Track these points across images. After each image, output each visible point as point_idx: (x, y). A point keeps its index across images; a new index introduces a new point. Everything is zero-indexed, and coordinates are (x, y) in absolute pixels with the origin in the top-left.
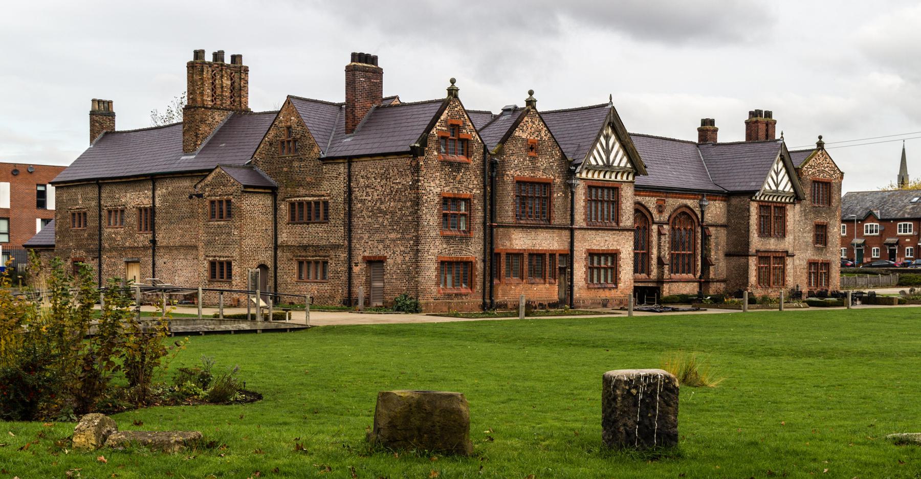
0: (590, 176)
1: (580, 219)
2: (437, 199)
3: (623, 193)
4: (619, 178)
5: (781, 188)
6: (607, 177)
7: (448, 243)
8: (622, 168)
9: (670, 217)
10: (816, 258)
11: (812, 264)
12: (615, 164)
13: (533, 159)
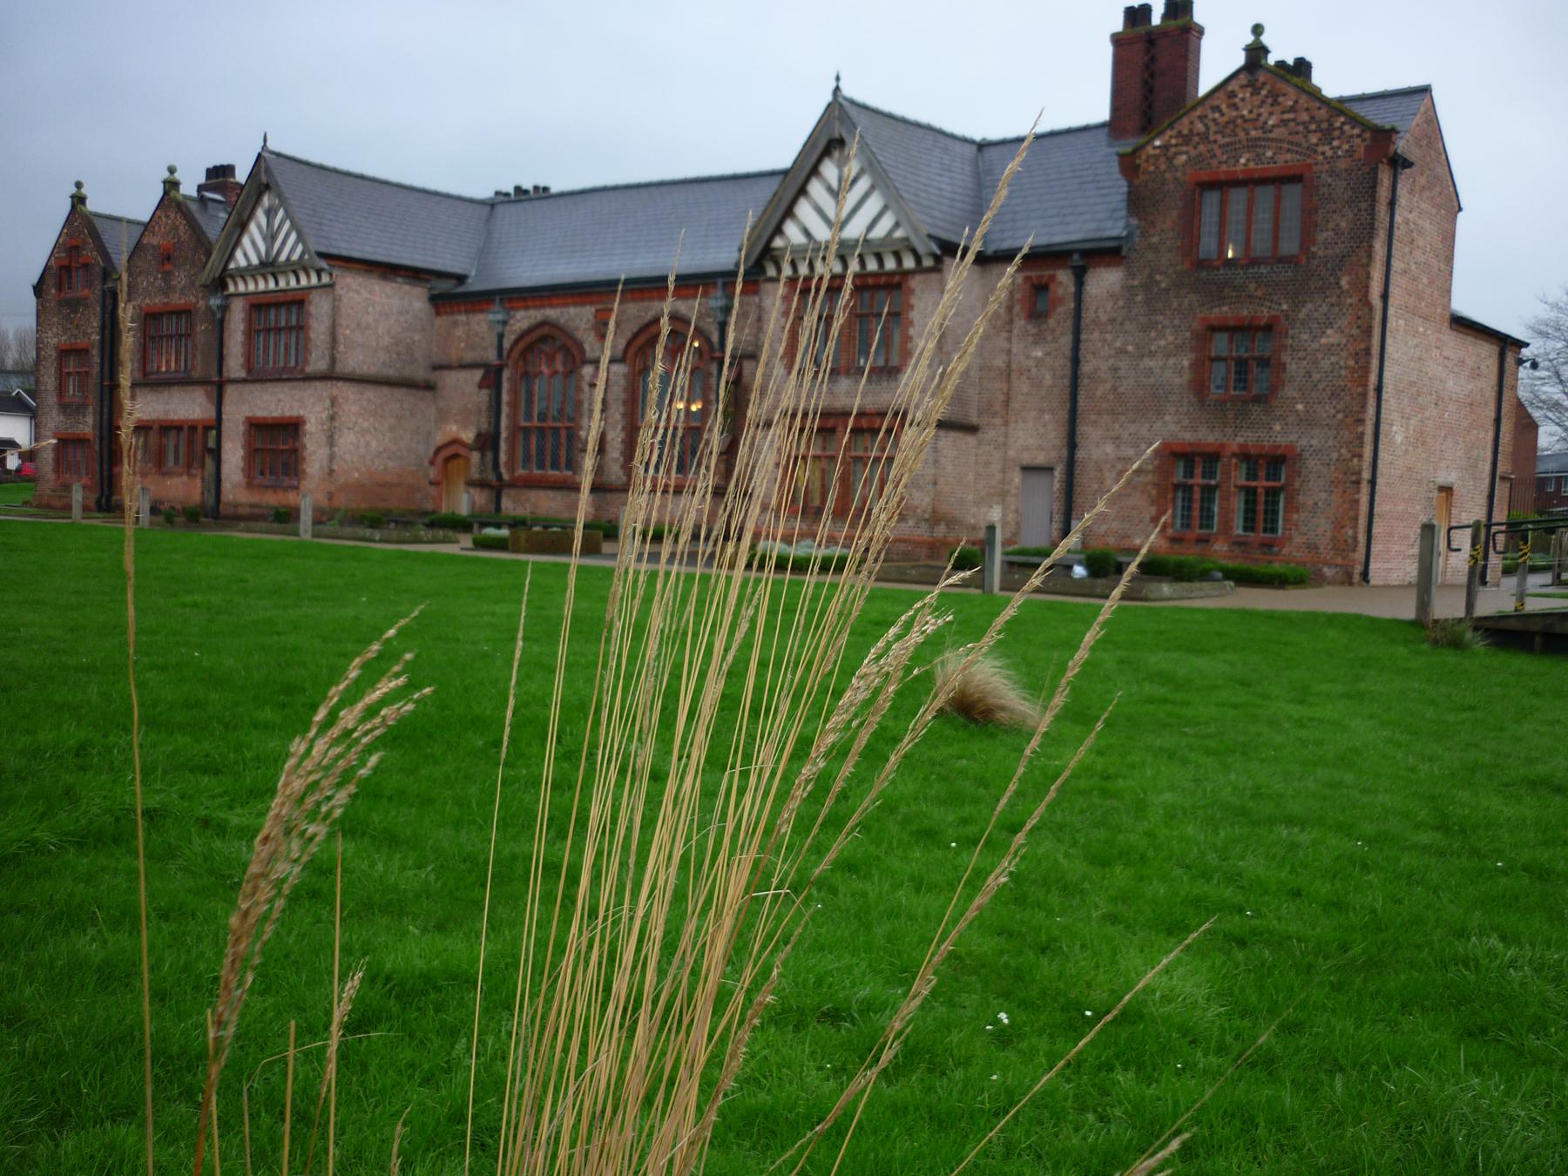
0: (251, 287)
1: (235, 365)
2: (54, 354)
3: (312, 309)
4: (304, 282)
5: (854, 230)
6: (282, 284)
7: (64, 413)
8: (294, 263)
9: (629, 344)
10: (1207, 436)
11: (1179, 456)
12: (283, 257)
13: (167, 276)
